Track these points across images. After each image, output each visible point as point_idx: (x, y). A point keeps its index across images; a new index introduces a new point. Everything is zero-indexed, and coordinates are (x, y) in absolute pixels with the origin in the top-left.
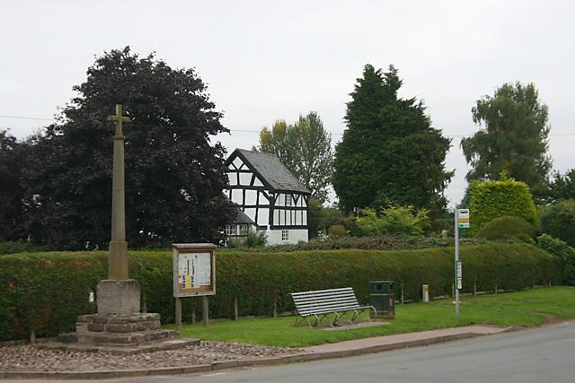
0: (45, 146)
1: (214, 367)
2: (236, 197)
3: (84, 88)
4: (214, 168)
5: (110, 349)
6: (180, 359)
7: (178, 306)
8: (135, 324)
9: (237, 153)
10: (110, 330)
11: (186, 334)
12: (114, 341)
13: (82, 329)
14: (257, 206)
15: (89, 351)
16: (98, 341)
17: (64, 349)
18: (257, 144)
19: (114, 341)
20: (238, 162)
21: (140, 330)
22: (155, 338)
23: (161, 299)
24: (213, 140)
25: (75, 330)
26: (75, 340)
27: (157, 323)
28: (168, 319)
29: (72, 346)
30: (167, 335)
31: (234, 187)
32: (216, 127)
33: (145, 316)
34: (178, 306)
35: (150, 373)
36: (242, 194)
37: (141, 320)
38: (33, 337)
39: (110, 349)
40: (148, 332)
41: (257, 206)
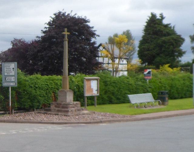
0: (35, 43)
1: (101, 122)
2: (100, 60)
3: (49, 24)
4: (94, 50)
5: (63, 114)
6: (18, 119)
7: (86, 99)
8: (72, 105)
9: (100, 45)
10: (63, 107)
11: (86, 111)
12: (64, 111)
13: (52, 107)
14: (108, 64)
15: (55, 114)
16: (58, 111)
17: (46, 113)
18: (107, 42)
19: (64, 111)
20: (101, 48)
21: (73, 107)
22: (79, 110)
23: (79, 96)
24: (93, 40)
25: (50, 107)
26: (50, 110)
27: (79, 105)
28: (82, 105)
29: (49, 112)
30: (83, 109)
31: (100, 57)
32: (93, 34)
33: (75, 103)
34: (86, 99)
35: (78, 123)
36: (103, 59)
37: (74, 104)
38: (35, 110)
39: (63, 114)
40: (76, 108)
41: (108, 64)
